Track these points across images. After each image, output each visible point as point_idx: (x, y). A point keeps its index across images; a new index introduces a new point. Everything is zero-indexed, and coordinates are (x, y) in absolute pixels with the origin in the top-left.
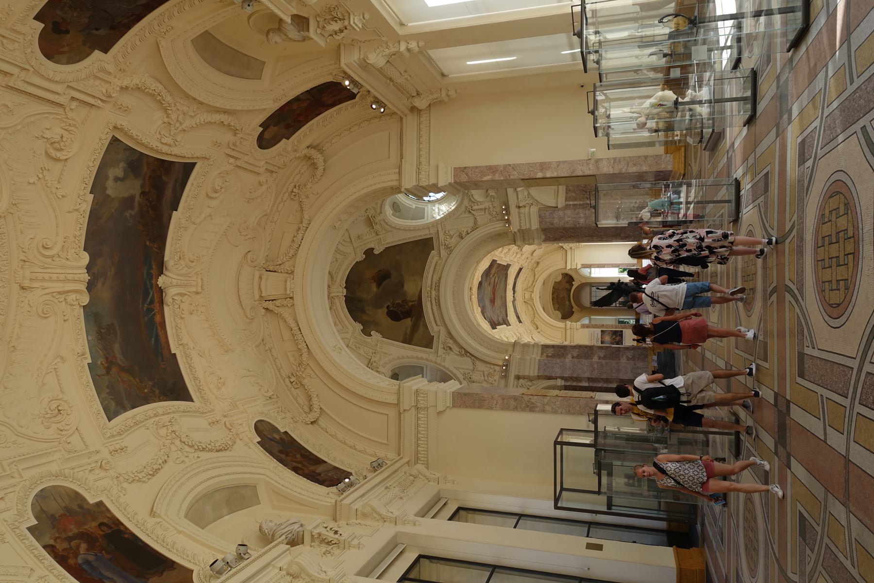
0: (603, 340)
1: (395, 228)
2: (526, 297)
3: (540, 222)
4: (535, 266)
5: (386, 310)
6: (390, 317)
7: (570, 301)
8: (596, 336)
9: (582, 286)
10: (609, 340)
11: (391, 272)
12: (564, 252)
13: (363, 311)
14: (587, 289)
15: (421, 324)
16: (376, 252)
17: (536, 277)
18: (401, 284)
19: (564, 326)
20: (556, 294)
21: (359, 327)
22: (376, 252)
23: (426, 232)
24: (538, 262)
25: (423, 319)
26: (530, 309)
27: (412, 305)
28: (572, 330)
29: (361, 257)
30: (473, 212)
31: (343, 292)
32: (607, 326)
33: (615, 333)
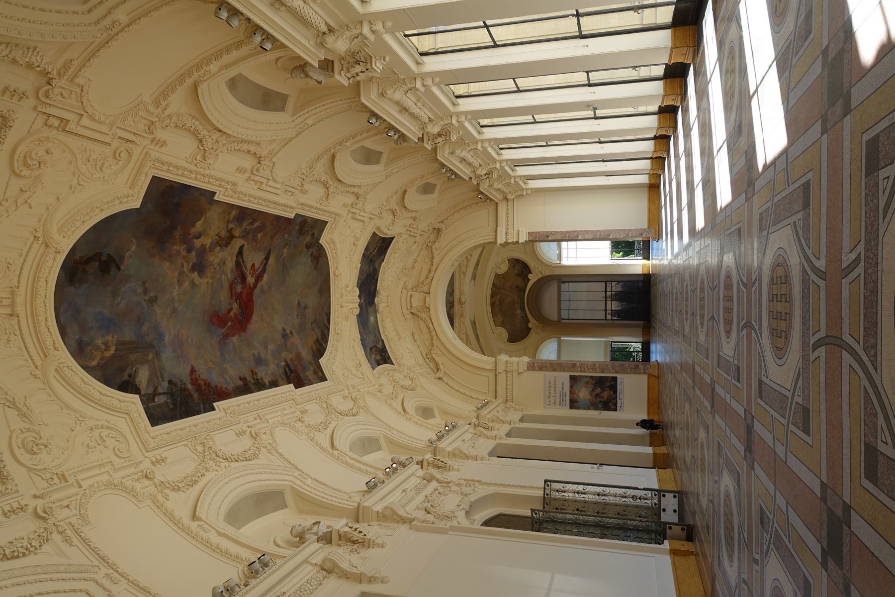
0: (575, 396)
2: (413, 305)
4: (432, 237)
7: (524, 309)
8: (559, 389)
9: (545, 281)
10: (588, 397)
12: (492, 208)
14: (554, 287)
17: (436, 260)
19: (491, 367)
20: (499, 296)
24: (439, 230)
26: (425, 330)
28: (509, 375)
32: (583, 366)
33: (600, 382)
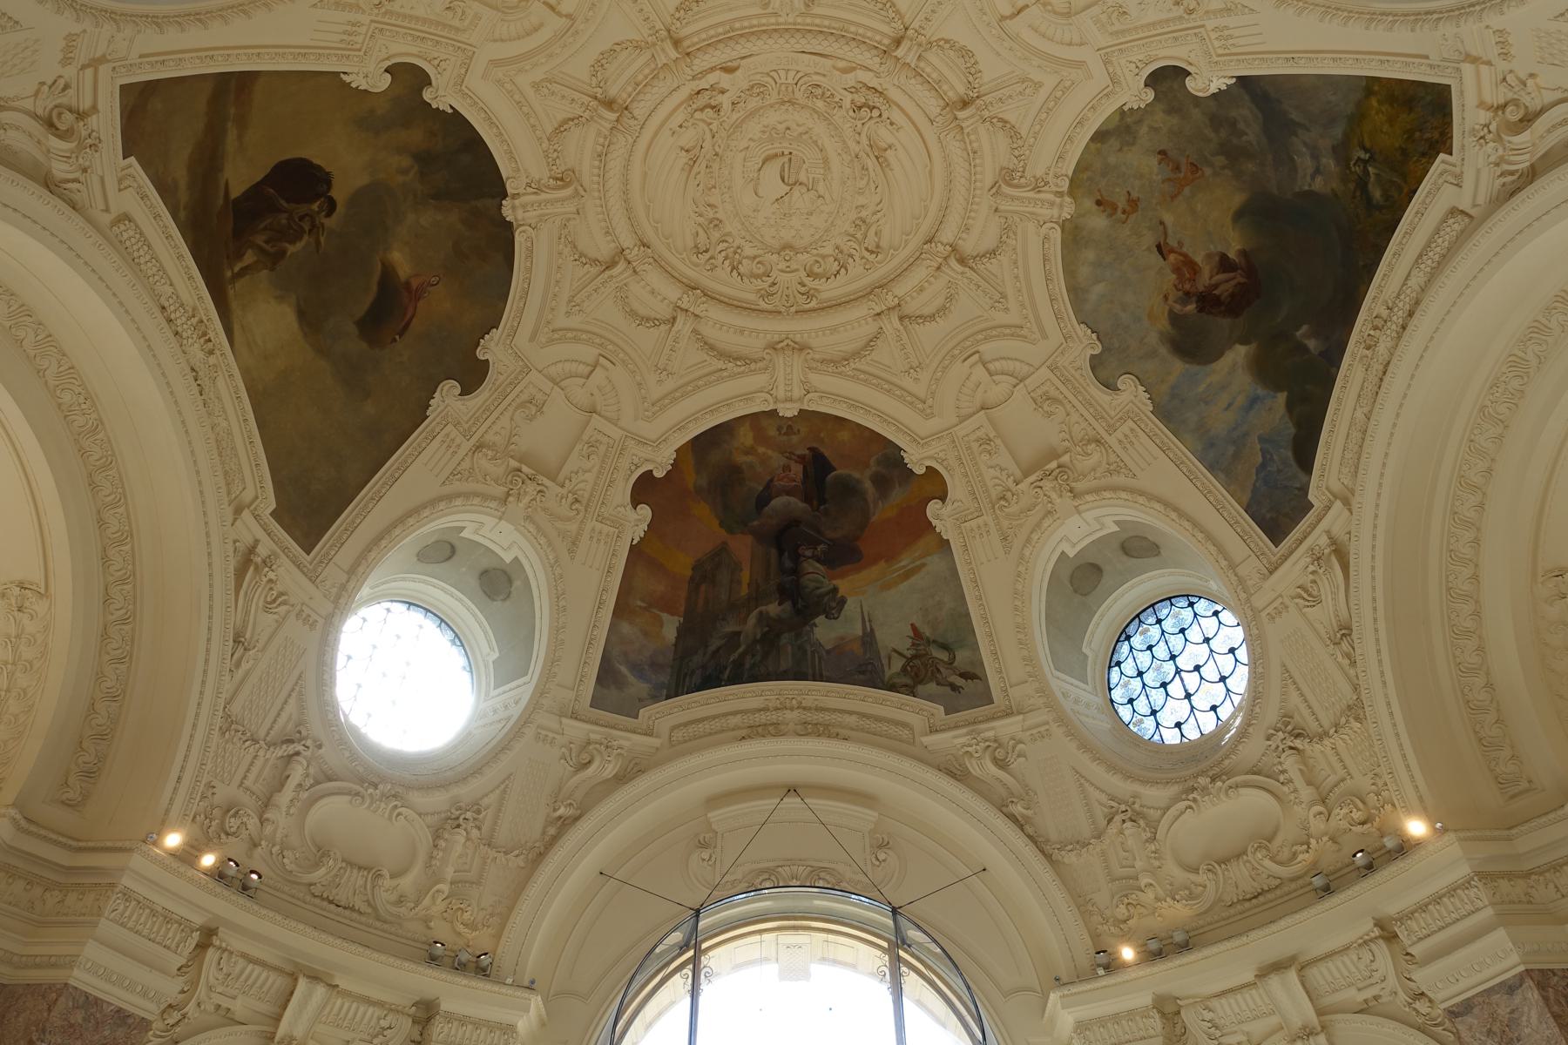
1: (449, 498)
3: (90, 1003)
5: (335, 193)
6: (319, 168)
11: (364, 345)
13: (425, 160)
15: (183, 196)
16: (450, 388)
18: (310, 319)
21: (440, 96)
22: (450, 388)
23: (345, 556)
25: (182, 214)
27: (239, 256)
29: (492, 348)
30: (282, 751)
31: (514, 208)
